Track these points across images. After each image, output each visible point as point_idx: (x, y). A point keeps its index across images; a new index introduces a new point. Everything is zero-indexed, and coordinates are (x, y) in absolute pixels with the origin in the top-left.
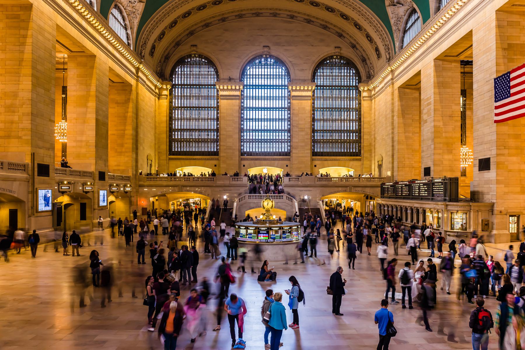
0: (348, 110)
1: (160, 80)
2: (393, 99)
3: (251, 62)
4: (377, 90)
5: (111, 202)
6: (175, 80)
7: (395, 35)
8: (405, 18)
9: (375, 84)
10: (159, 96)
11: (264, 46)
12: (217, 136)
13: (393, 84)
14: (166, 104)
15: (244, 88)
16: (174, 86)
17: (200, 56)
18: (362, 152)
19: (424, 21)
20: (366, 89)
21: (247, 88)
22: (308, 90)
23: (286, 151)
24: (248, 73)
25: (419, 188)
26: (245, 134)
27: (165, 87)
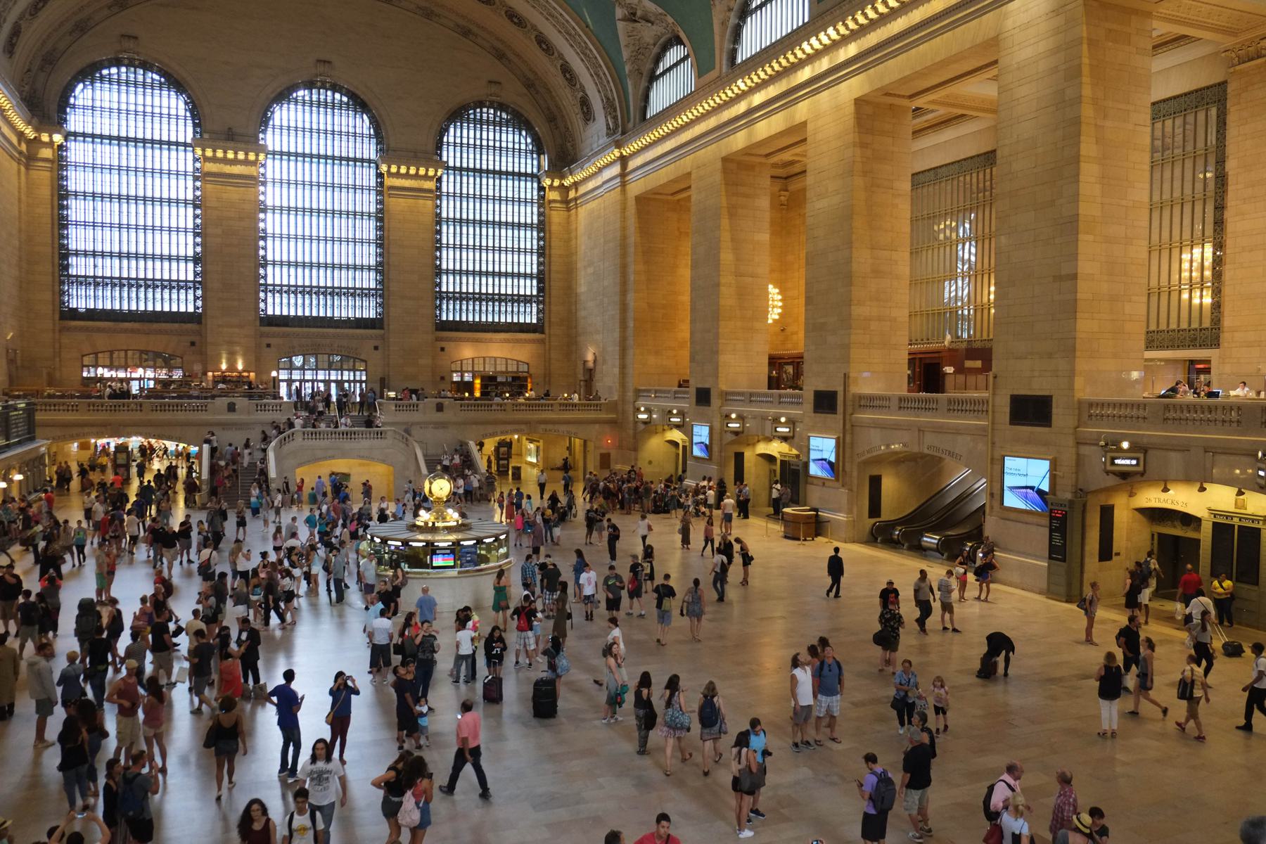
1: (35, 121)
2: (624, 218)
3: (283, 96)
4: (582, 190)
8: (656, 50)
9: (579, 176)
10: (29, 160)
11: (319, 61)
12: (196, 274)
13: (623, 184)
14: (48, 182)
16: (68, 135)
17: (146, 66)
18: (546, 325)
19: (701, 71)
20: (556, 183)
22: (426, 177)
24: (277, 122)
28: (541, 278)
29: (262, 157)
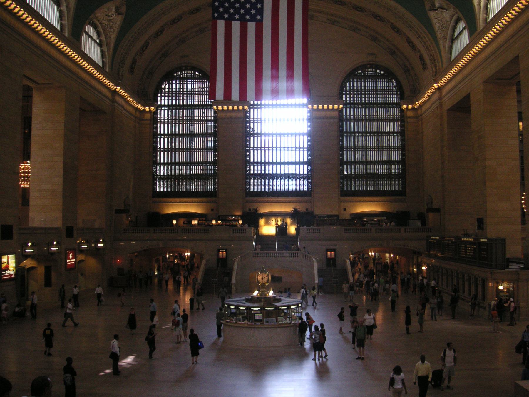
0: (389, 134)
4: (424, 109)
5: (81, 261)
6: (161, 100)
7: (441, 43)
8: (452, 24)
13: (441, 105)
15: (250, 108)
17: (194, 69)
18: (407, 191)
20: (410, 106)
21: (254, 108)
23: (306, 189)
25: (466, 247)
26: (252, 167)
27: (147, 109)
28: (402, 162)
29: (246, 107)
